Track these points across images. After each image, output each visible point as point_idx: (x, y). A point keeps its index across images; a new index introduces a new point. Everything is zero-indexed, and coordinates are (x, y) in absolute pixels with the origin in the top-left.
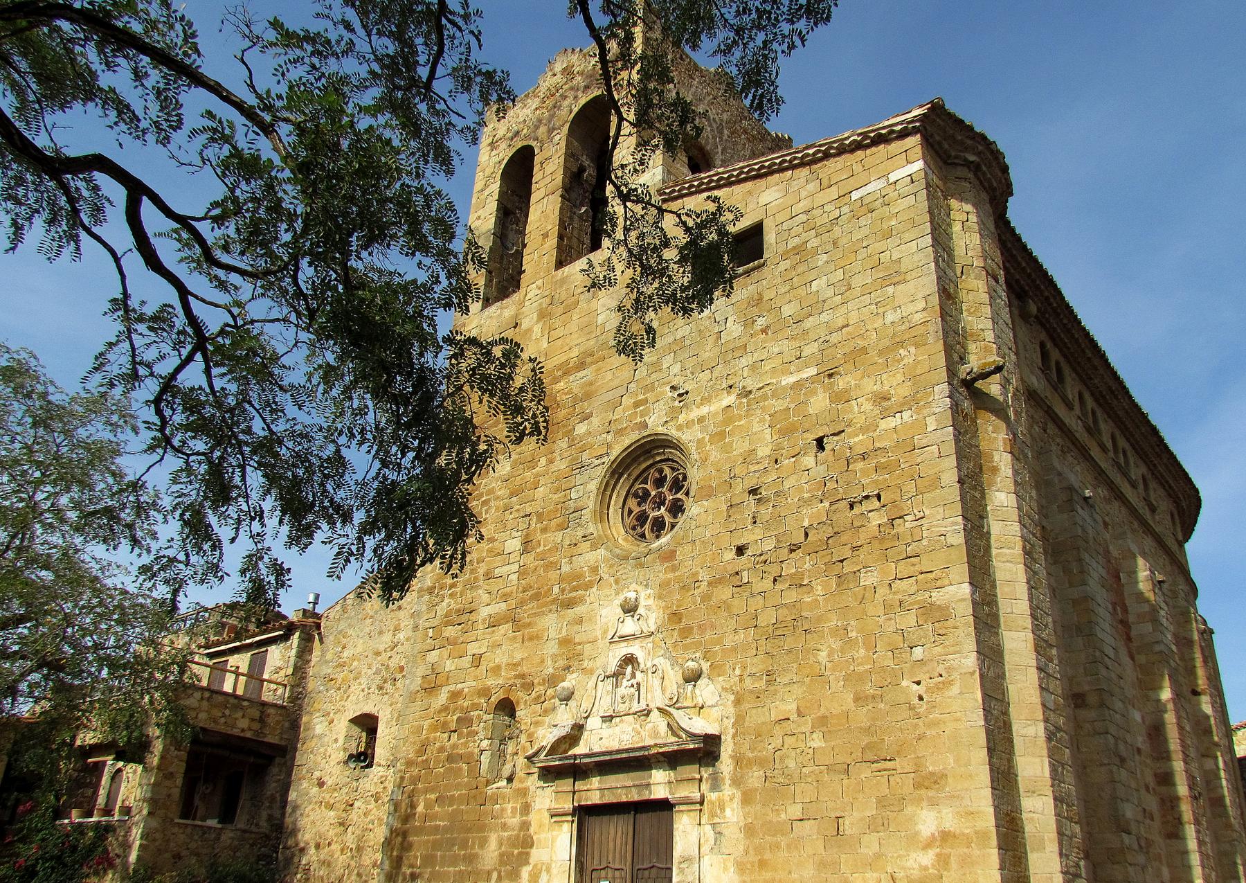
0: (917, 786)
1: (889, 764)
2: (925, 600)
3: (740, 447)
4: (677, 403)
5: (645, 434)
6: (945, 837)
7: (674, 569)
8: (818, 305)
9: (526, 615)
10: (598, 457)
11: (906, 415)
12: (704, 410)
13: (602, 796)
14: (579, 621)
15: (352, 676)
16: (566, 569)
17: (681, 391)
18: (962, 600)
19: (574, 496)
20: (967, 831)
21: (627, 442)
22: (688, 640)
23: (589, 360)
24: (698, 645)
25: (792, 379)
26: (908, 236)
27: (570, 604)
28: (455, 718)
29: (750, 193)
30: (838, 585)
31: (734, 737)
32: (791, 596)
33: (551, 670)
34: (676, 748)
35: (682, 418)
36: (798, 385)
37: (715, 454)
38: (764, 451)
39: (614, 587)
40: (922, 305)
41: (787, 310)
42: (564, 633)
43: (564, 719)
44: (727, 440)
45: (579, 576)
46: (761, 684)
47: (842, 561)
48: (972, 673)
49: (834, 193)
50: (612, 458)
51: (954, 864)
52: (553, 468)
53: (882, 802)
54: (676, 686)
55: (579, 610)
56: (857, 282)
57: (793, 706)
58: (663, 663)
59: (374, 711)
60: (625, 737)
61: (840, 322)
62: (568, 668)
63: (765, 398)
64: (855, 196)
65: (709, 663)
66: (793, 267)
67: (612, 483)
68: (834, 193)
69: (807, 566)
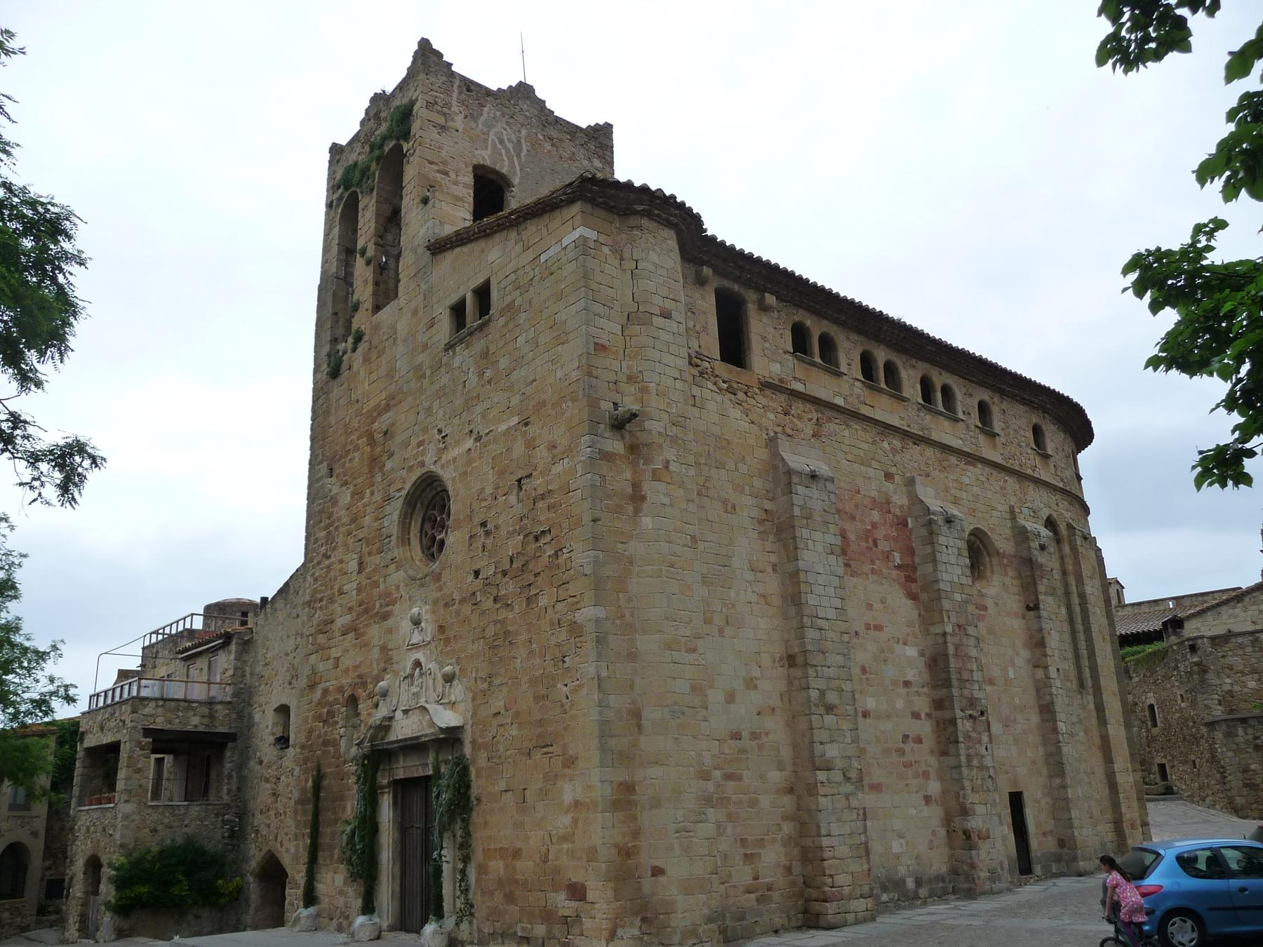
0: (565, 766)
1: (550, 749)
2: (571, 620)
6: (577, 804)
7: (440, 589)
11: (566, 461)
14: (390, 631)
15: (274, 673)
17: (443, 434)
18: (590, 620)
20: (587, 800)
21: (414, 478)
23: (392, 403)
25: (503, 427)
26: (572, 299)
27: (385, 617)
28: (326, 710)
30: (528, 605)
31: (472, 726)
34: (434, 737)
36: (507, 432)
38: (489, 490)
39: (409, 603)
40: (576, 364)
41: (503, 363)
43: (383, 712)
46: (485, 686)
47: (530, 585)
48: (593, 679)
49: (530, 254)
50: (406, 492)
51: (580, 825)
53: (546, 779)
55: (390, 622)
56: (542, 340)
57: (502, 704)
59: (287, 703)
60: (415, 727)
63: (489, 442)
64: (543, 258)
66: (506, 324)
67: (410, 511)
68: (530, 254)
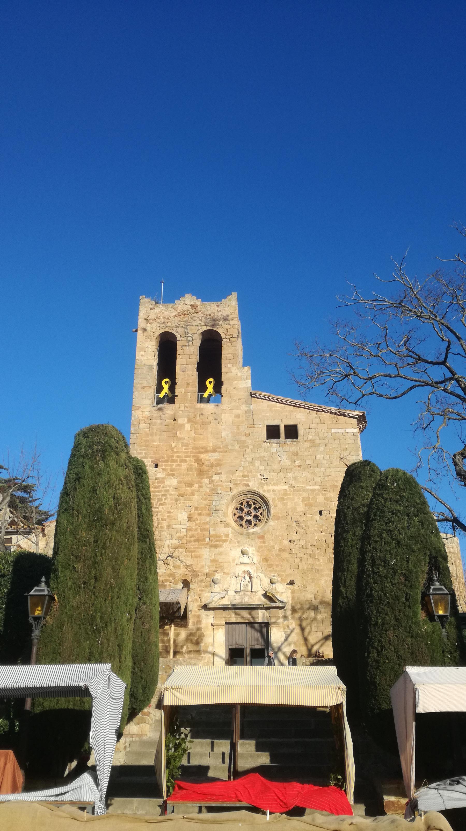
3: (290, 505)
4: (263, 481)
5: (248, 489)
7: (264, 542)
8: (319, 465)
9: (192, 547)
10: (226, 491)
12: (275, 488)
13: (236, 620)
16: (212, 532)
19: (214, 503)
21: (240, 490)
22: (271, 569)
24: (275, 571)
27: (216, 546)
29: (292, 411)
32: (311, 560)
33: (208, 571)
35: (265, 488)
36: (313, 490)
37: (280, 505)
42: (213, 557)
44: (285, 501)
45: (220, 536)
50: (233, 494)
52: (202, 489)
54: (267, 584)
55: (221, 550)
58: (262, 576)
61: (328, 474)
62: (216, 571)
64: (333, 431)
65: (280, 578)
69: (317, 552)
